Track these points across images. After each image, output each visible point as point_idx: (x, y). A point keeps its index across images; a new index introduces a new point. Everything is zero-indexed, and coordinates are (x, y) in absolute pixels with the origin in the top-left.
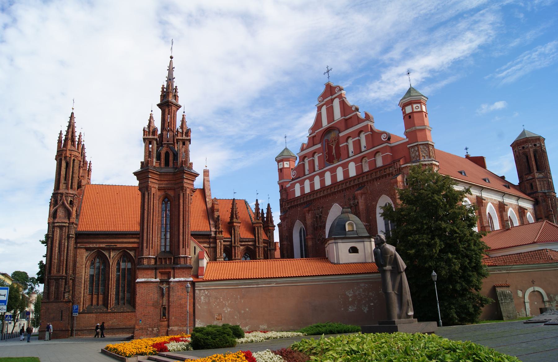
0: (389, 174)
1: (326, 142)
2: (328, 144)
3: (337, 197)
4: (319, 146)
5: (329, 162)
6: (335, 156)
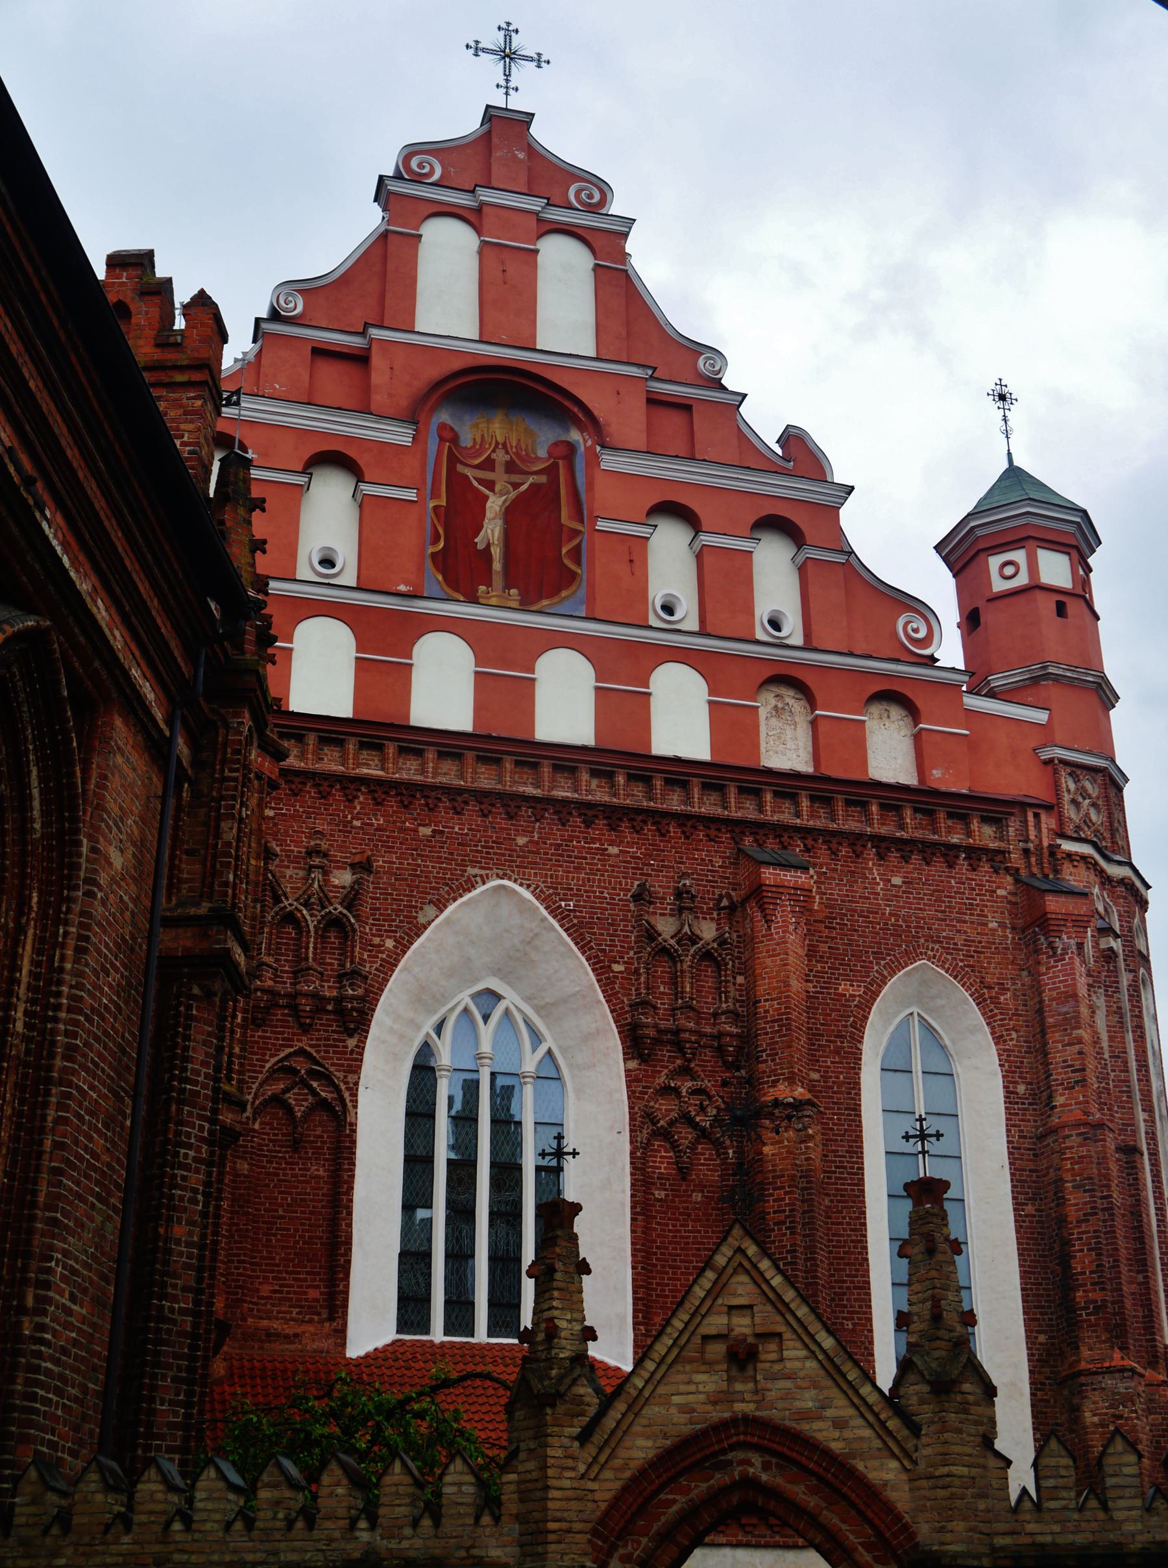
0: (975, 854)
1: (442, 439)
2: (453, 460)
3: (521, 841)
4: (401, 435)
6: (497, 566)
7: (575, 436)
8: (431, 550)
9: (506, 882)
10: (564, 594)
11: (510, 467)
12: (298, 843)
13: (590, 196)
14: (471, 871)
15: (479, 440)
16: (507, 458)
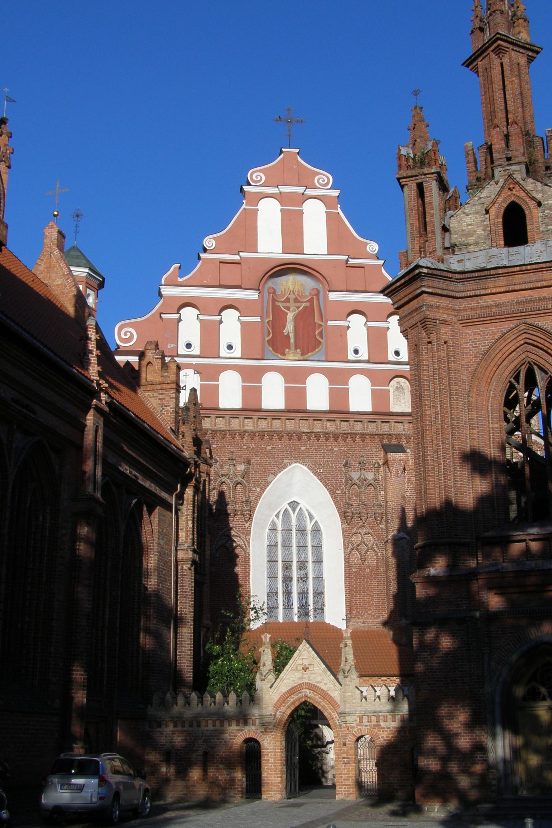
1: (269, 293)
2: (274, 300)
3: (303, 448)
4: (253, 295)
5: (273, 349)
6: (292, 341)
7: (320, 287)
8: (267, 339)
9: (298, 464)
10: (317, 350)
11: (296, 300)
12: (225, 456)
13: (324, 181)
14: (285, 461)
15: (283, 291)
16: (294, 297)
